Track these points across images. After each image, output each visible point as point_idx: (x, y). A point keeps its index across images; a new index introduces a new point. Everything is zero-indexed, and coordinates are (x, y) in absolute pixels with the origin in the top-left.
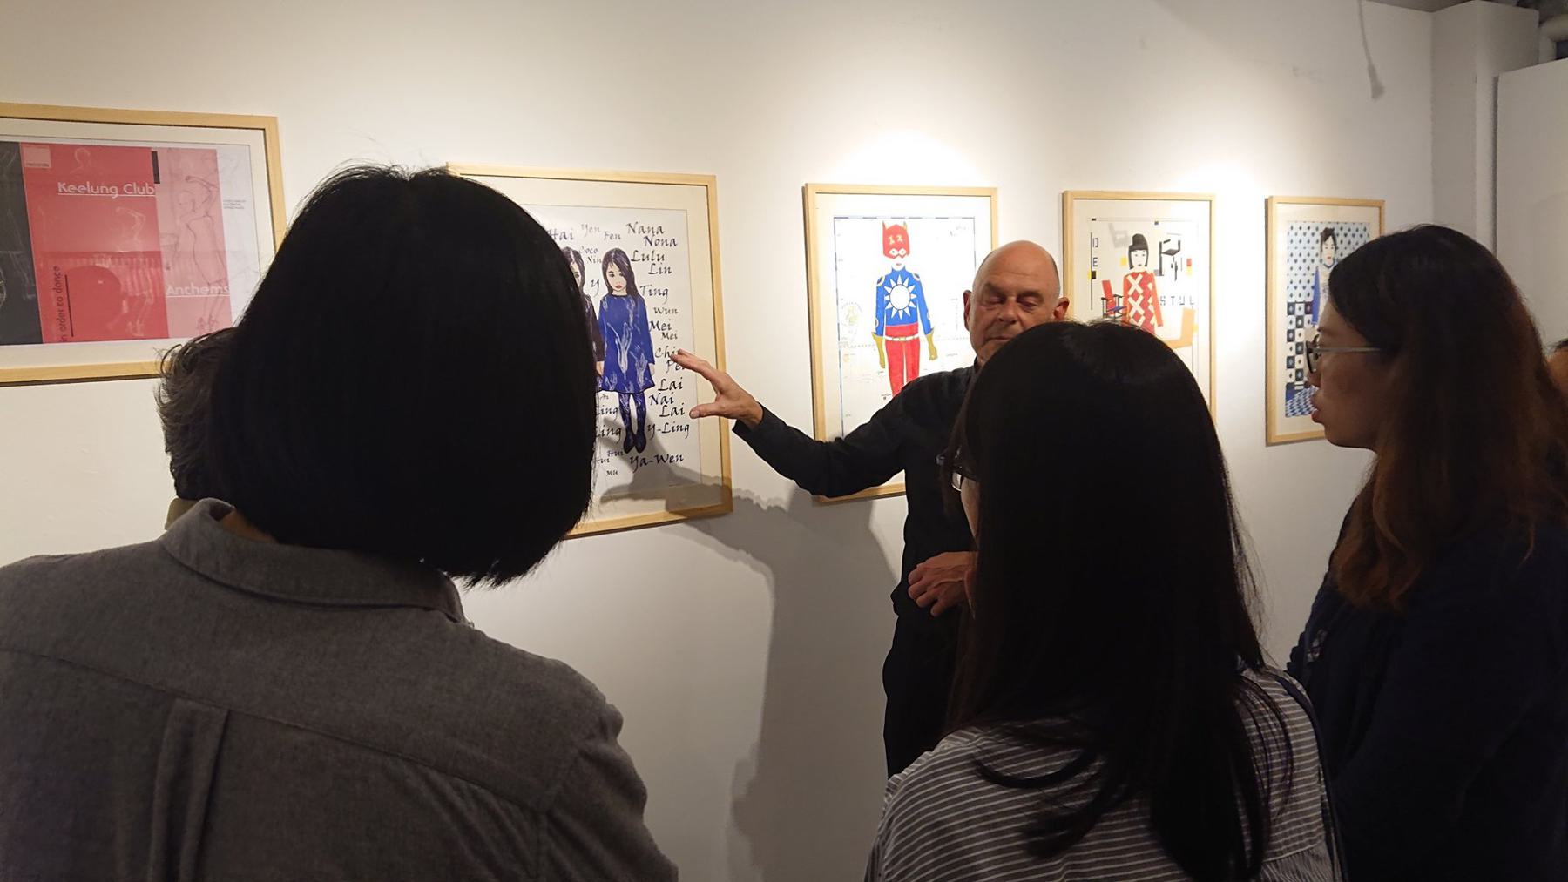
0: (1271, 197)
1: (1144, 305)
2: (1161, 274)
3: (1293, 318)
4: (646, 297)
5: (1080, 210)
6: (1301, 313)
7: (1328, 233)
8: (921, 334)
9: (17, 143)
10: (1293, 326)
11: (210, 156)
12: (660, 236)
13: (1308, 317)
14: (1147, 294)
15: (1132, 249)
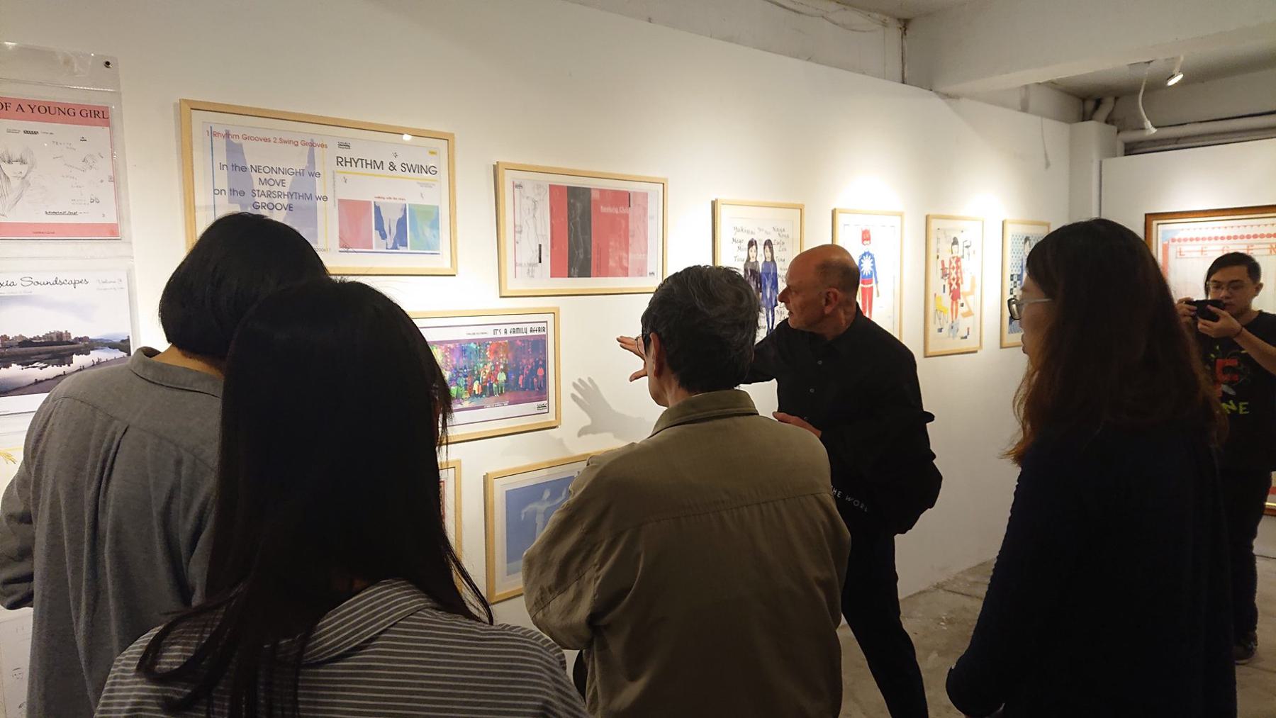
0: (1005, 220)
1: (957, 273)
2: (963, 257)
3: (1012, 282)
4: (777, 263)
5: (934, 224)
6: (1015, 279)
7: (1027, 239)
8: (874, 284)
9: (590, 189)
10: (1012, 287)
11: (645, 195)
12: (784, 233)
13: (1018, 282)
14: (958, 267)
15: (953, 244)
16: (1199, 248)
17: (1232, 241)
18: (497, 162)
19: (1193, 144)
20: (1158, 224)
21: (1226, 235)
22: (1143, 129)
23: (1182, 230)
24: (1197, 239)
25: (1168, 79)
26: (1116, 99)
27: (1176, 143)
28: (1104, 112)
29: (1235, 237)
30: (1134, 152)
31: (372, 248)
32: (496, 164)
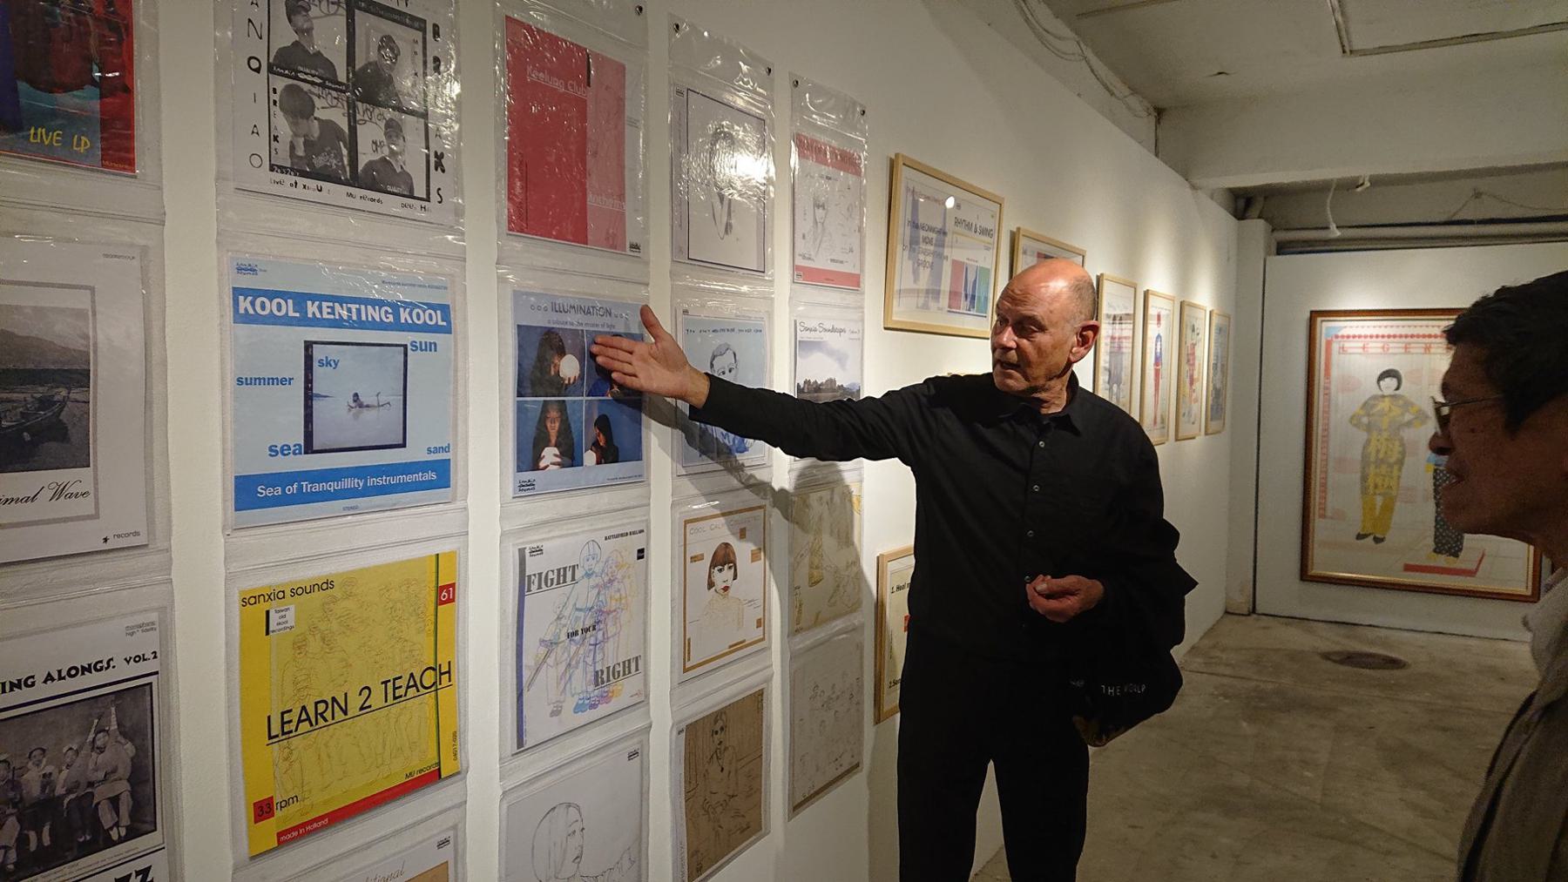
16: (1361, 345)
17: (1392, 339)
18: (1019, 229)
19: (1352, 247)
20: (1322, 321)
21: (1386, 334)
22: (1327, 228)
23: (1345, 327)
24: (1360, 337)
25: (1357, 187)
26: (1266, 198)
27: (1325, 245)
28: (1255, 211)
29: (1395, 336)
30: (1292, 250)
31: (960, 308)
32: (1015, 230)
